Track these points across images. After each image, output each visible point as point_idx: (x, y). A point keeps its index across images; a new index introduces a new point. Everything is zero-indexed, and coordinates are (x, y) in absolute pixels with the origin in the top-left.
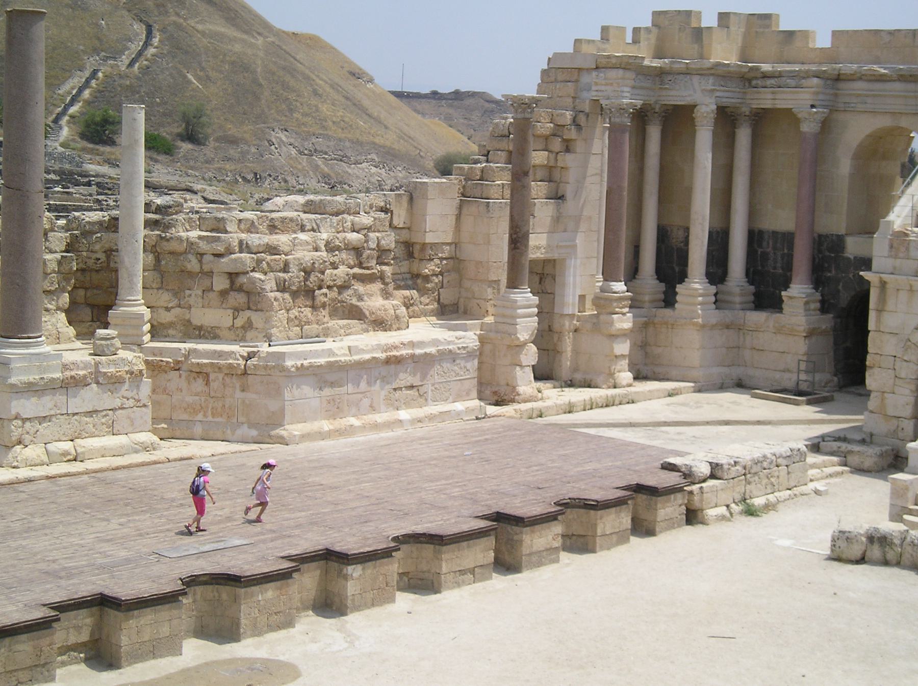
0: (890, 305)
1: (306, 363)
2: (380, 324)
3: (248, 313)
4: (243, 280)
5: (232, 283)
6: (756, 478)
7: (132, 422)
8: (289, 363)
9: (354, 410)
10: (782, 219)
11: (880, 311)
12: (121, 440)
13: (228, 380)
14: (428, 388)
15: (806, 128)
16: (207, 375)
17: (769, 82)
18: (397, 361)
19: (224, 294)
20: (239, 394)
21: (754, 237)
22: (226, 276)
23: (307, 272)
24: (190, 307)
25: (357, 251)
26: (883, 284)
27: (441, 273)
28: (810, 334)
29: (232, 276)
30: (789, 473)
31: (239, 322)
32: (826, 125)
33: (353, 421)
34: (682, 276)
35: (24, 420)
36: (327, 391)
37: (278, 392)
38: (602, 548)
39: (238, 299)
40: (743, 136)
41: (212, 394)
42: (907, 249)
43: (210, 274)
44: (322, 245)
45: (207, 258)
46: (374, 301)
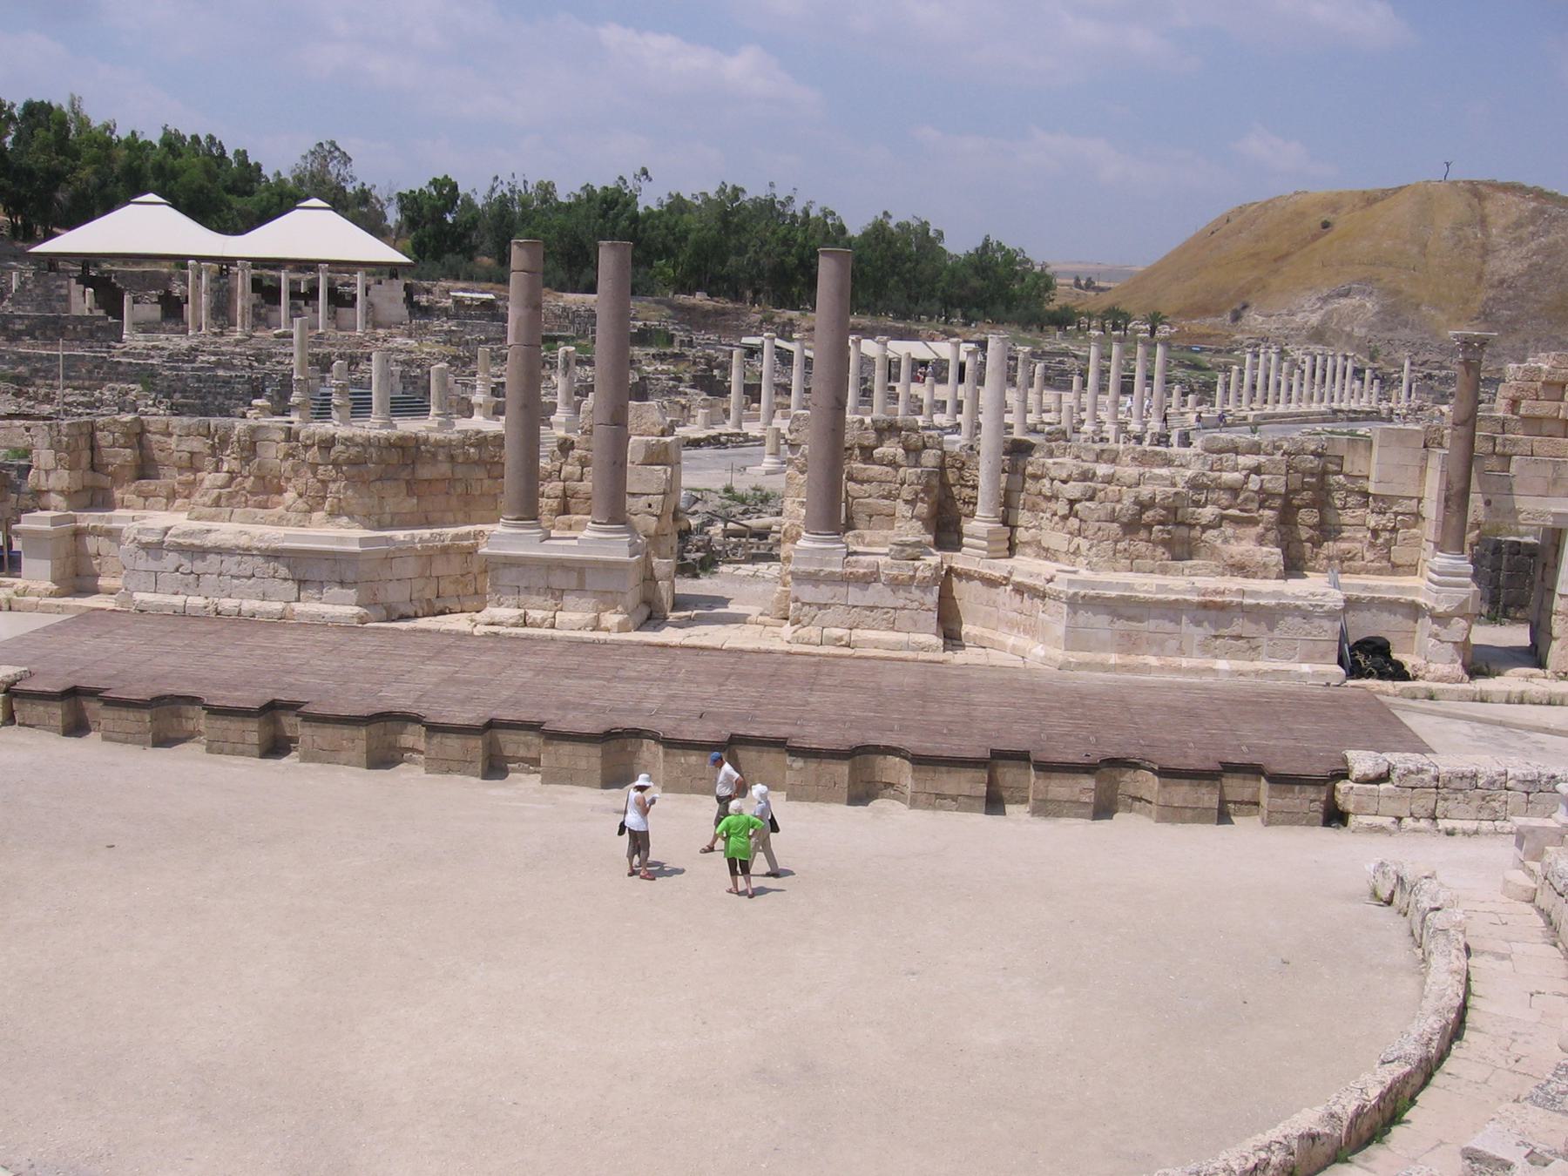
1: (1092, 593)
2: (1240, 568)
4: (1077, 506)
6: (1460, 796)
7: (915, 623)
9: (1155, 649)
12: (902, 637)
14: (1263, 641)
18: (1223, 607)
19: (1065, 518)
25: (1234, 490)
27: (1394, 530)
29: (1072, 502)
30: (1528, 802)
33: (1152, 661)
35: (804, 604)
36: (1121, 625)
39: (1073, 523)
46: (1244, 546)
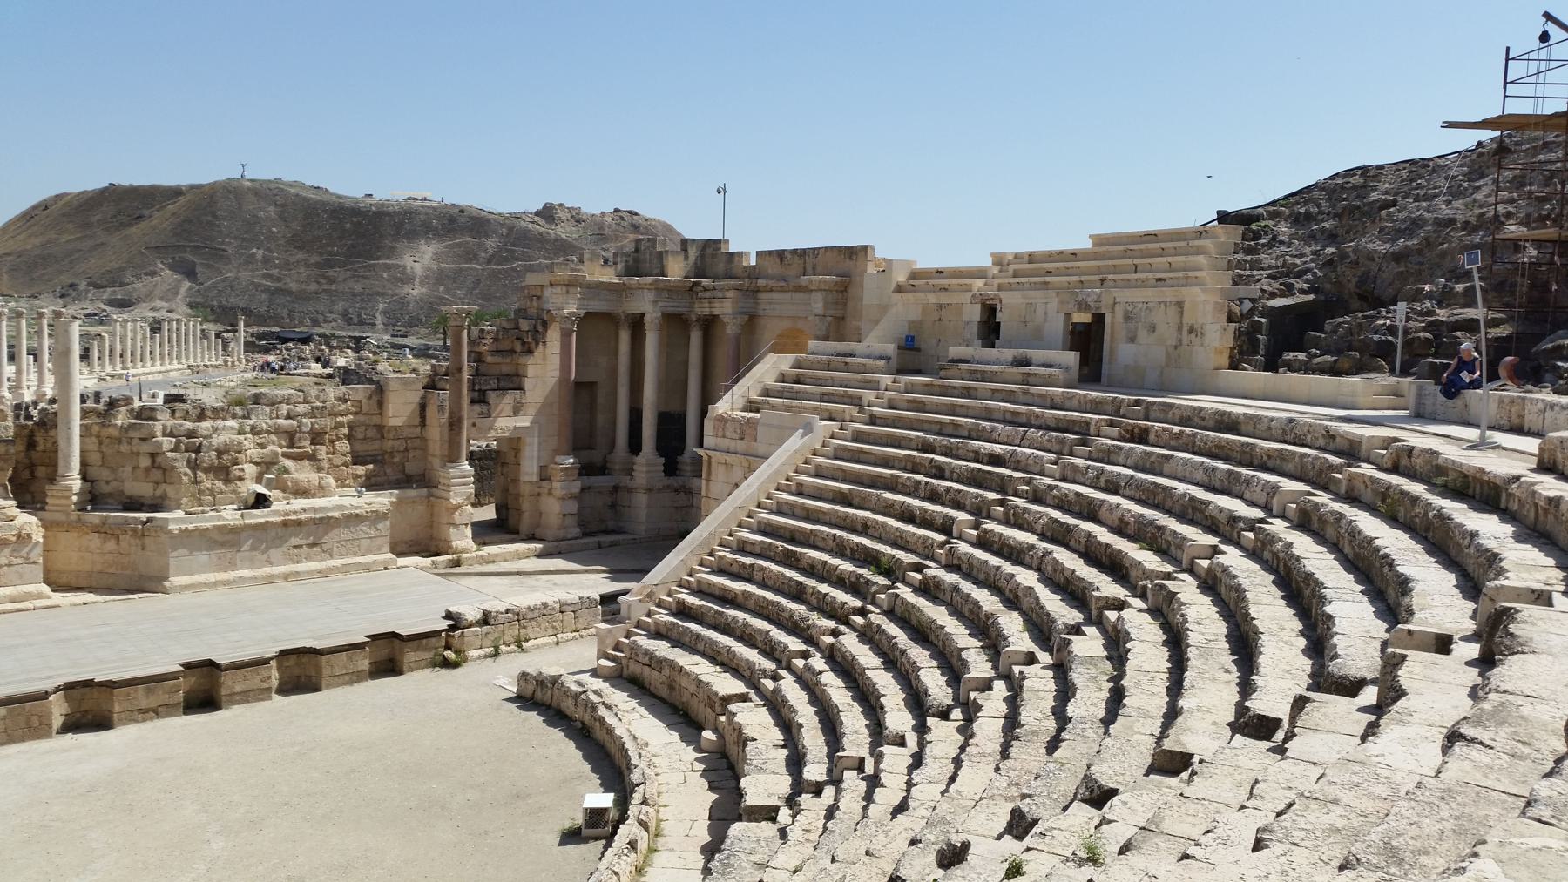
1: (190, 527)
5: (154, 462)
7: (21, 576)
8: (171, 527)
11: (708, 480)
17: (708, 294)
19: (147, 470)
23: (220, 453)
29: (153, 455)
31: (158, 493)
38: (328, 687)
44: (248, 429)
45: (136, 441)
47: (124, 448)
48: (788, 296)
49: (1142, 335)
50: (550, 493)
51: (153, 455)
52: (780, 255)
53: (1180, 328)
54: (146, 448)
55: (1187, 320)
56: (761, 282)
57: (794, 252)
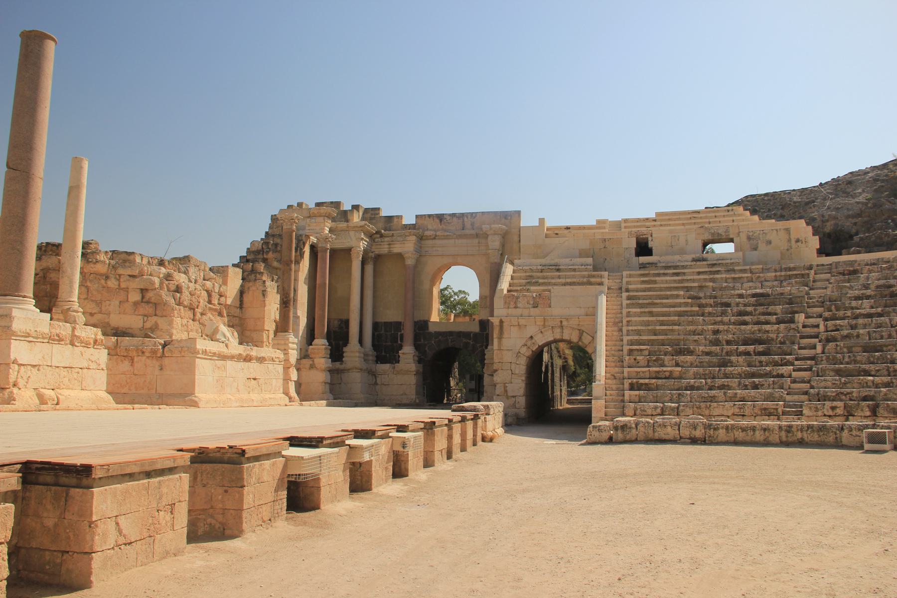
0: (505, 335)
3: (155, 319)
5: (143, 297)
10: (391, 315)
11: (500, 338)
13: (149, 362)
15: (410, 262)
16: (132, 359)
17: (386, 239)
19: (136, 304)
20: (157, 372)
21: (376, 326)
22: (139, 291)
24: (109, 314)
26: (501, 322)
28: (417, 373)
29: (143, 291)
31: (148, 325)
32: (418, 261)
34: (346, 341)
37: (190, 370)
40: (369, 268)
41: (136, 372)
42: (515, 303)
43: (126, 290)
47: (112, 283)
48: (451, 242)
49: (762, 247)
50: (312, 367)
51: (143, 291)
52: (440, 217)
53: (789, 240)
54: (136, 284)
55: (794, 237)
56: (427, 233)
57: (453, 215)
